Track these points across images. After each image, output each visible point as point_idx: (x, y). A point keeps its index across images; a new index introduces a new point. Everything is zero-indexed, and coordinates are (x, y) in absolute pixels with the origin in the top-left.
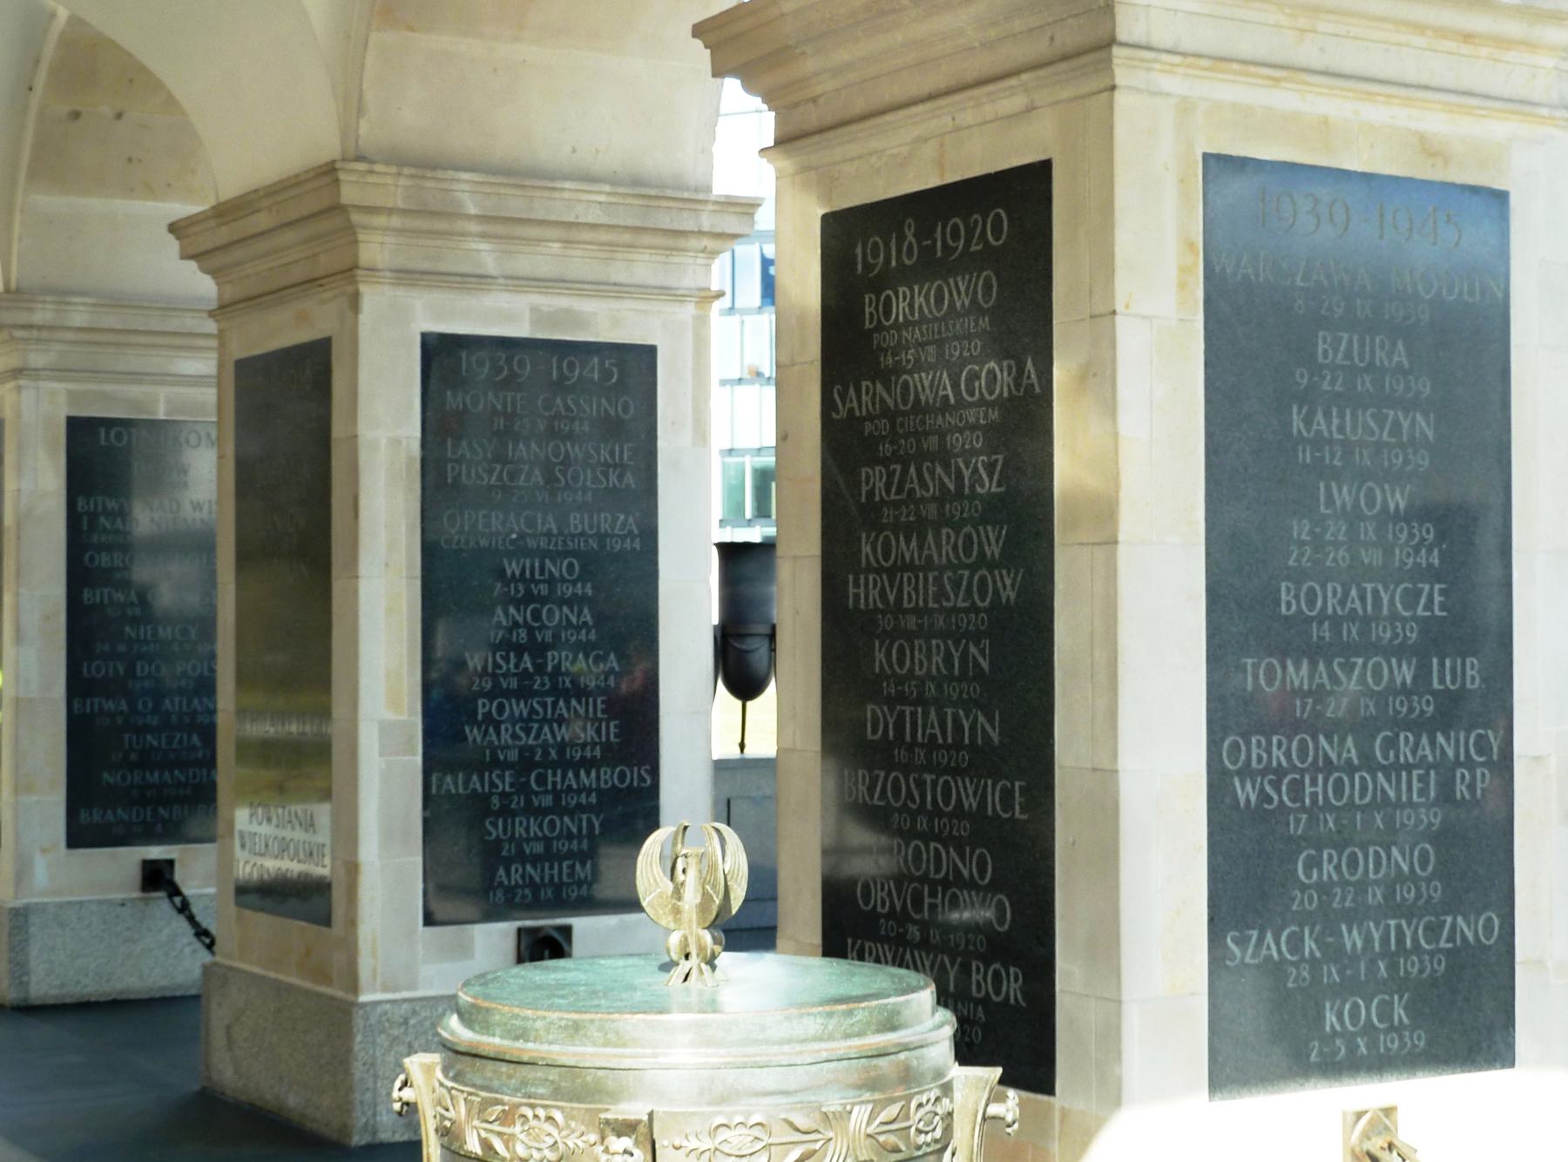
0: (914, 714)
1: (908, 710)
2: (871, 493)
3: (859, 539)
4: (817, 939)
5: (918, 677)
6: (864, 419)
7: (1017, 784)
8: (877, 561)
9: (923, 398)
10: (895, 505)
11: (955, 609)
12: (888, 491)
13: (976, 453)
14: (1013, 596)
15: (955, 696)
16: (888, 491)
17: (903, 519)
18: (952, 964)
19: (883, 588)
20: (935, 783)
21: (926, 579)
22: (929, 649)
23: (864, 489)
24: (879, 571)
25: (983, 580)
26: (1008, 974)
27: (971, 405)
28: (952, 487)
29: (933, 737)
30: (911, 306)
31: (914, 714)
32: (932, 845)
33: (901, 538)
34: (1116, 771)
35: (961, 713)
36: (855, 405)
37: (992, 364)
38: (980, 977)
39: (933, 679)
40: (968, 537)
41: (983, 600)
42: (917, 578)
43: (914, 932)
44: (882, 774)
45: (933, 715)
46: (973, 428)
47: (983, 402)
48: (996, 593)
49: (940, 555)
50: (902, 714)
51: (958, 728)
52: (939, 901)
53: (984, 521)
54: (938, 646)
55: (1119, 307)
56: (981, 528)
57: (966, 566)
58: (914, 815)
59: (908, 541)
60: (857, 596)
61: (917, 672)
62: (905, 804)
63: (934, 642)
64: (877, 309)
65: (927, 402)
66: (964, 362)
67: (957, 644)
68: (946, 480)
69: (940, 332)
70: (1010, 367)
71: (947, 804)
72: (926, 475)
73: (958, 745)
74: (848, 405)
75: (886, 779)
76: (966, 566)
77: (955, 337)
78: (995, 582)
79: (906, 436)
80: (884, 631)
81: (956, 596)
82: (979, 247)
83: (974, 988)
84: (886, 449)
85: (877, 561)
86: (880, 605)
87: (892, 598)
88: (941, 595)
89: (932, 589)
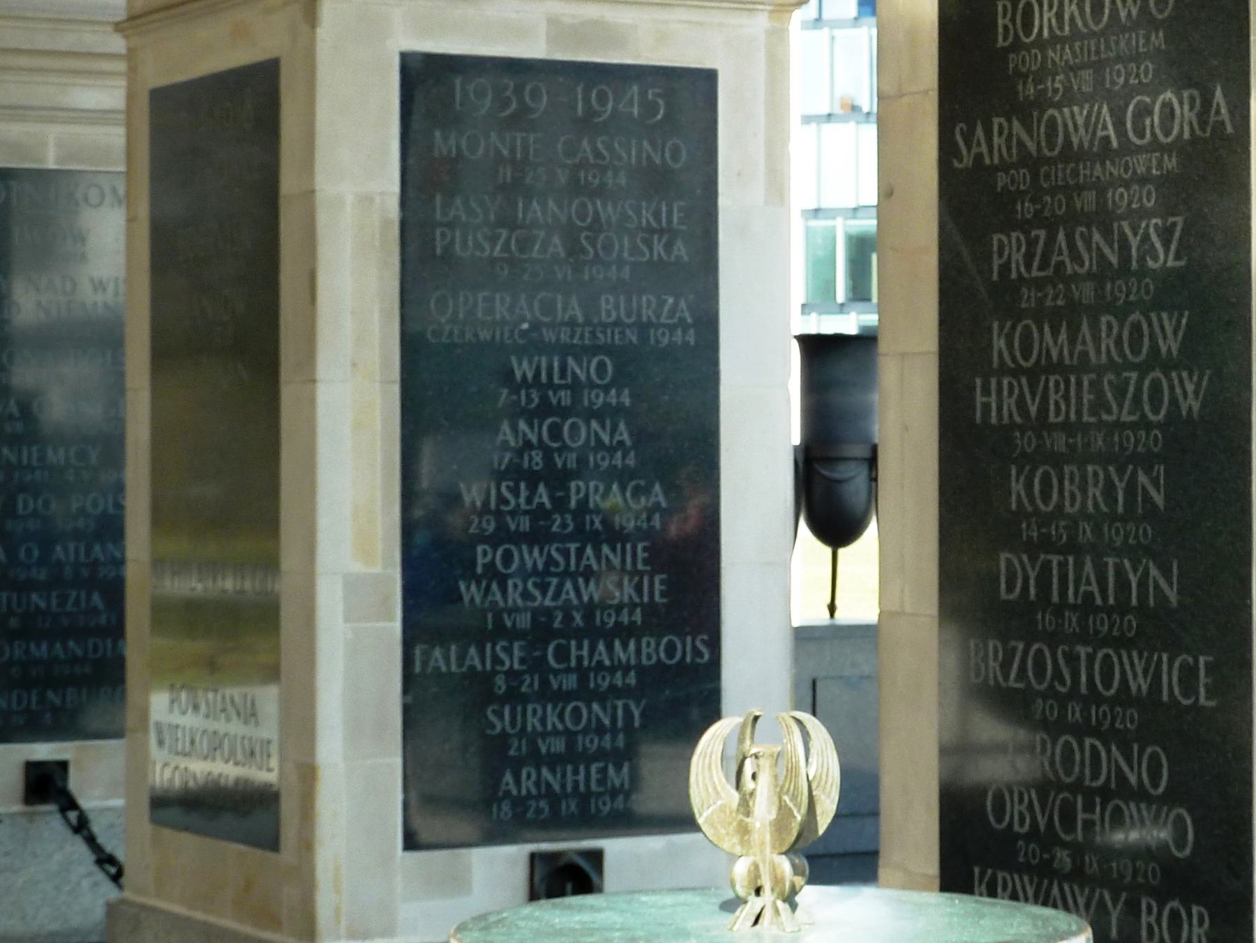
0: (1063, 565)
1: (1055, 559)
2: (1006, 268)
3: (990, 330)
4: (932, 868)
6: (997, 169)
7: (1202, 660)
8: (1014, 359)
9: (1075, 140)
10: (1039, 284)
11: (1119, 425)
12: (1028, 266)
13: (1148, 214)
14: (1196, 406)
15: (1119, 542)
16: (1028, 266)
17: (1049, 303)
18: (1115, 901)
19: (1021, 395)
20: (1091, 658)
21: (1079, 384)
22: (1084, 478)
23: (996, 263)
24: (1016, 372)
25: (1156, 388)
26: (1190, 915)
27: (1140, 149)
28: (1114, 260)
29: (1089, 596)
30: (1059, 16)
31: (1063, 565)
32: (1088, 742)
33: (1047, 329)
35: (1127, 563)
36: (984, 149)
37: (1169, 95)
39: (1088, 518)
40: (1136, 328)
41: (1156, 411)
42: (1067, 382)
43: (1063, 858)
44: (1021, 646)
45: (1088, 567)
46: (1143, 180)
47: (1155, 145)
48: (1174, 402)
49: (1098, 351)
50: (1046, 567)
52: (1097, 816)
53: (1158, 305)
54: (1096, 474)
56: (1153, 316)
57: (1134, 367)
58: (1063, 701)
59: (1055, 332)
60: (986, 407)
61: (1068, 509)
62: (1051, 686)
63: (1090, 468)
64: (1013, 20)
65: (1081, 145)
66: (1129, 91)
67: (1121, 471)
68: (1107, 251)
69: (1098, 52)
70: (1192, 99)
71: (1108, 686)
72: (1080, 244)
73: (1123, 607)
74: (974, 150)
76: (1134, 367)
77: (1119, 59)
78: (1172, 388)
79: (1053, 191)
81: (1121, 406)
84: (1026, 209)
85: (1014, 359)
86: (1018, 419)
87: (1033, 410)
88: (1100, 404)
89: (1087, 397)
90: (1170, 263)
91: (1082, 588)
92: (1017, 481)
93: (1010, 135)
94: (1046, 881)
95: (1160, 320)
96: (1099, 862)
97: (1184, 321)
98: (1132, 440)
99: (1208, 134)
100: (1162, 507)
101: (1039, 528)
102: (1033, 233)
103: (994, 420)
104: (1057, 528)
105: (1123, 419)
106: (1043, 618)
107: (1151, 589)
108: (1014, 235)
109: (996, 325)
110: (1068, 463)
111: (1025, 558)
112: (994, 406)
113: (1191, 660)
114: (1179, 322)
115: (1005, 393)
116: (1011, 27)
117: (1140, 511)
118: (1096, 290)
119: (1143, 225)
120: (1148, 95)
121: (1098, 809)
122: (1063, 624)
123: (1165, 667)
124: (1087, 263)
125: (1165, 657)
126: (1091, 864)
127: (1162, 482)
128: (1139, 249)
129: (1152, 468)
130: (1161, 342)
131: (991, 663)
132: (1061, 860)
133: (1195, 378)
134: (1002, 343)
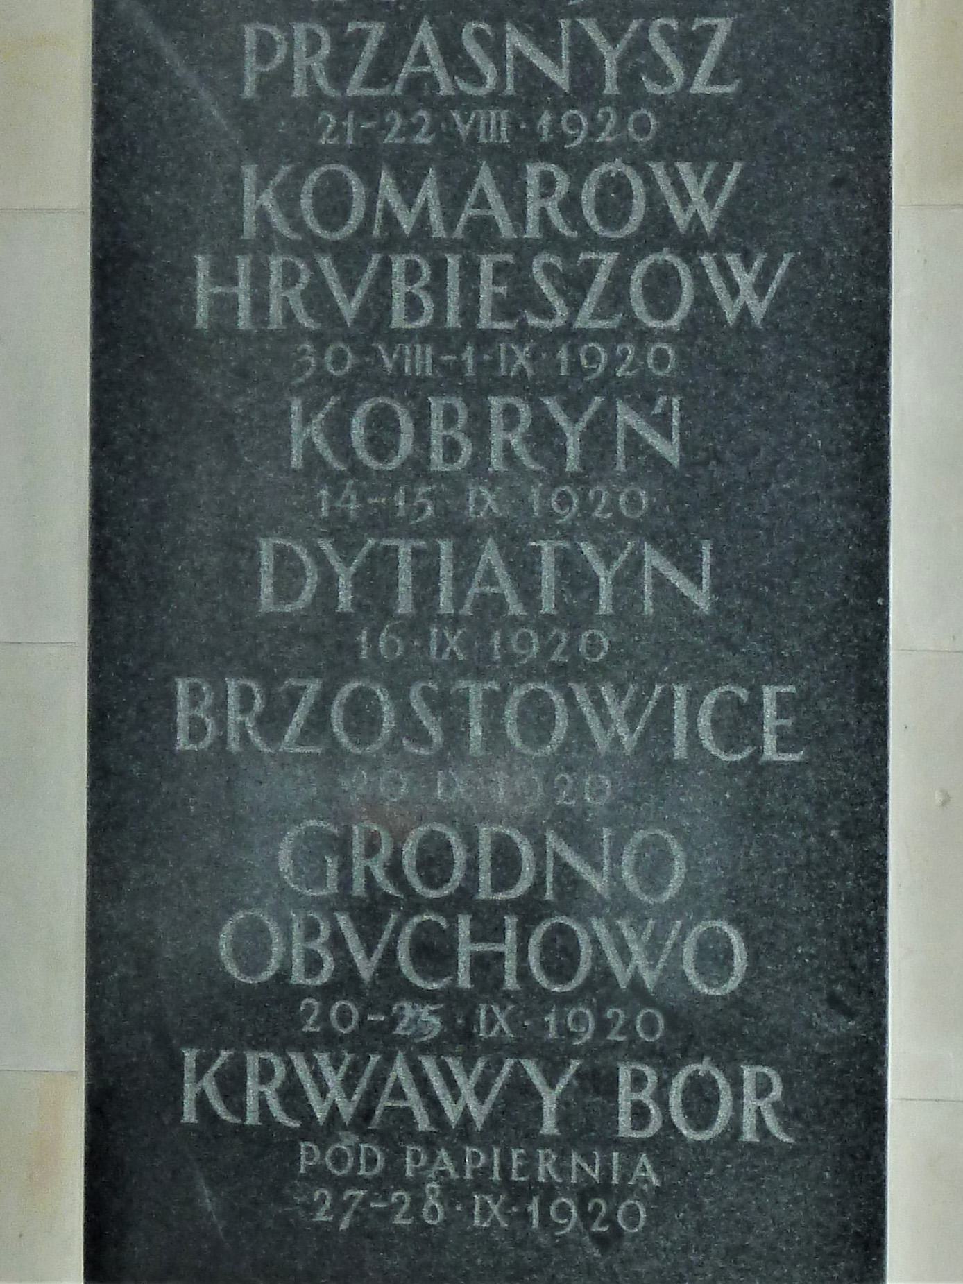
3: (236, 179)
5: (443, 477)
7: (768, 692)
10: (364, 108)
11: (569, 334)
14: (758, 310)
20: (495, 702)
21: (470, 272)
24: (309, 247)
28: (561, 78)
29: (492, 606)
35: (587, 549)
38: (645, 1096)
48: (705, 298)
49: (519, 218)
51: (573, 574)
52: (509, 945)
53: (667, 150)
57: (610, 245)
67: (574, 407)
72: (473, 49)
75: (324, 700)
80: (321, 378)
85: (299, 225)
86: (307, 322)
88: (520, 298)
90: (700, 86)
91: (474, 591)
92: (306, 420)
94: (374, 1059)
96: (511, 1020)
97: (732, 178)
98: (604, 357)
100: (676, 462)
101: (362, 499)
102: (351, 27)
104: (410, 496)
105: (578, 325)
106: (373, 640)
107: (648, 589)
108: (300, 30)
109: (250, 173)
110: (439, 392)
111: (326, 546)
112: (244, 301)
115: (275, 279)
117: (621, 467)
118: (514, 124)
119: (634, 25)
121: (510, 935)
122: (426, 646)
123: (680, 705)
124: (491, 81)
125: (680, 692)
126: (491, 1023)
127: (675, 422)
128: (621, 63)
129: (651, 400)
130: (675, 208)
131: (234, 716)
132: (415, 1020)
133: (757, 265)
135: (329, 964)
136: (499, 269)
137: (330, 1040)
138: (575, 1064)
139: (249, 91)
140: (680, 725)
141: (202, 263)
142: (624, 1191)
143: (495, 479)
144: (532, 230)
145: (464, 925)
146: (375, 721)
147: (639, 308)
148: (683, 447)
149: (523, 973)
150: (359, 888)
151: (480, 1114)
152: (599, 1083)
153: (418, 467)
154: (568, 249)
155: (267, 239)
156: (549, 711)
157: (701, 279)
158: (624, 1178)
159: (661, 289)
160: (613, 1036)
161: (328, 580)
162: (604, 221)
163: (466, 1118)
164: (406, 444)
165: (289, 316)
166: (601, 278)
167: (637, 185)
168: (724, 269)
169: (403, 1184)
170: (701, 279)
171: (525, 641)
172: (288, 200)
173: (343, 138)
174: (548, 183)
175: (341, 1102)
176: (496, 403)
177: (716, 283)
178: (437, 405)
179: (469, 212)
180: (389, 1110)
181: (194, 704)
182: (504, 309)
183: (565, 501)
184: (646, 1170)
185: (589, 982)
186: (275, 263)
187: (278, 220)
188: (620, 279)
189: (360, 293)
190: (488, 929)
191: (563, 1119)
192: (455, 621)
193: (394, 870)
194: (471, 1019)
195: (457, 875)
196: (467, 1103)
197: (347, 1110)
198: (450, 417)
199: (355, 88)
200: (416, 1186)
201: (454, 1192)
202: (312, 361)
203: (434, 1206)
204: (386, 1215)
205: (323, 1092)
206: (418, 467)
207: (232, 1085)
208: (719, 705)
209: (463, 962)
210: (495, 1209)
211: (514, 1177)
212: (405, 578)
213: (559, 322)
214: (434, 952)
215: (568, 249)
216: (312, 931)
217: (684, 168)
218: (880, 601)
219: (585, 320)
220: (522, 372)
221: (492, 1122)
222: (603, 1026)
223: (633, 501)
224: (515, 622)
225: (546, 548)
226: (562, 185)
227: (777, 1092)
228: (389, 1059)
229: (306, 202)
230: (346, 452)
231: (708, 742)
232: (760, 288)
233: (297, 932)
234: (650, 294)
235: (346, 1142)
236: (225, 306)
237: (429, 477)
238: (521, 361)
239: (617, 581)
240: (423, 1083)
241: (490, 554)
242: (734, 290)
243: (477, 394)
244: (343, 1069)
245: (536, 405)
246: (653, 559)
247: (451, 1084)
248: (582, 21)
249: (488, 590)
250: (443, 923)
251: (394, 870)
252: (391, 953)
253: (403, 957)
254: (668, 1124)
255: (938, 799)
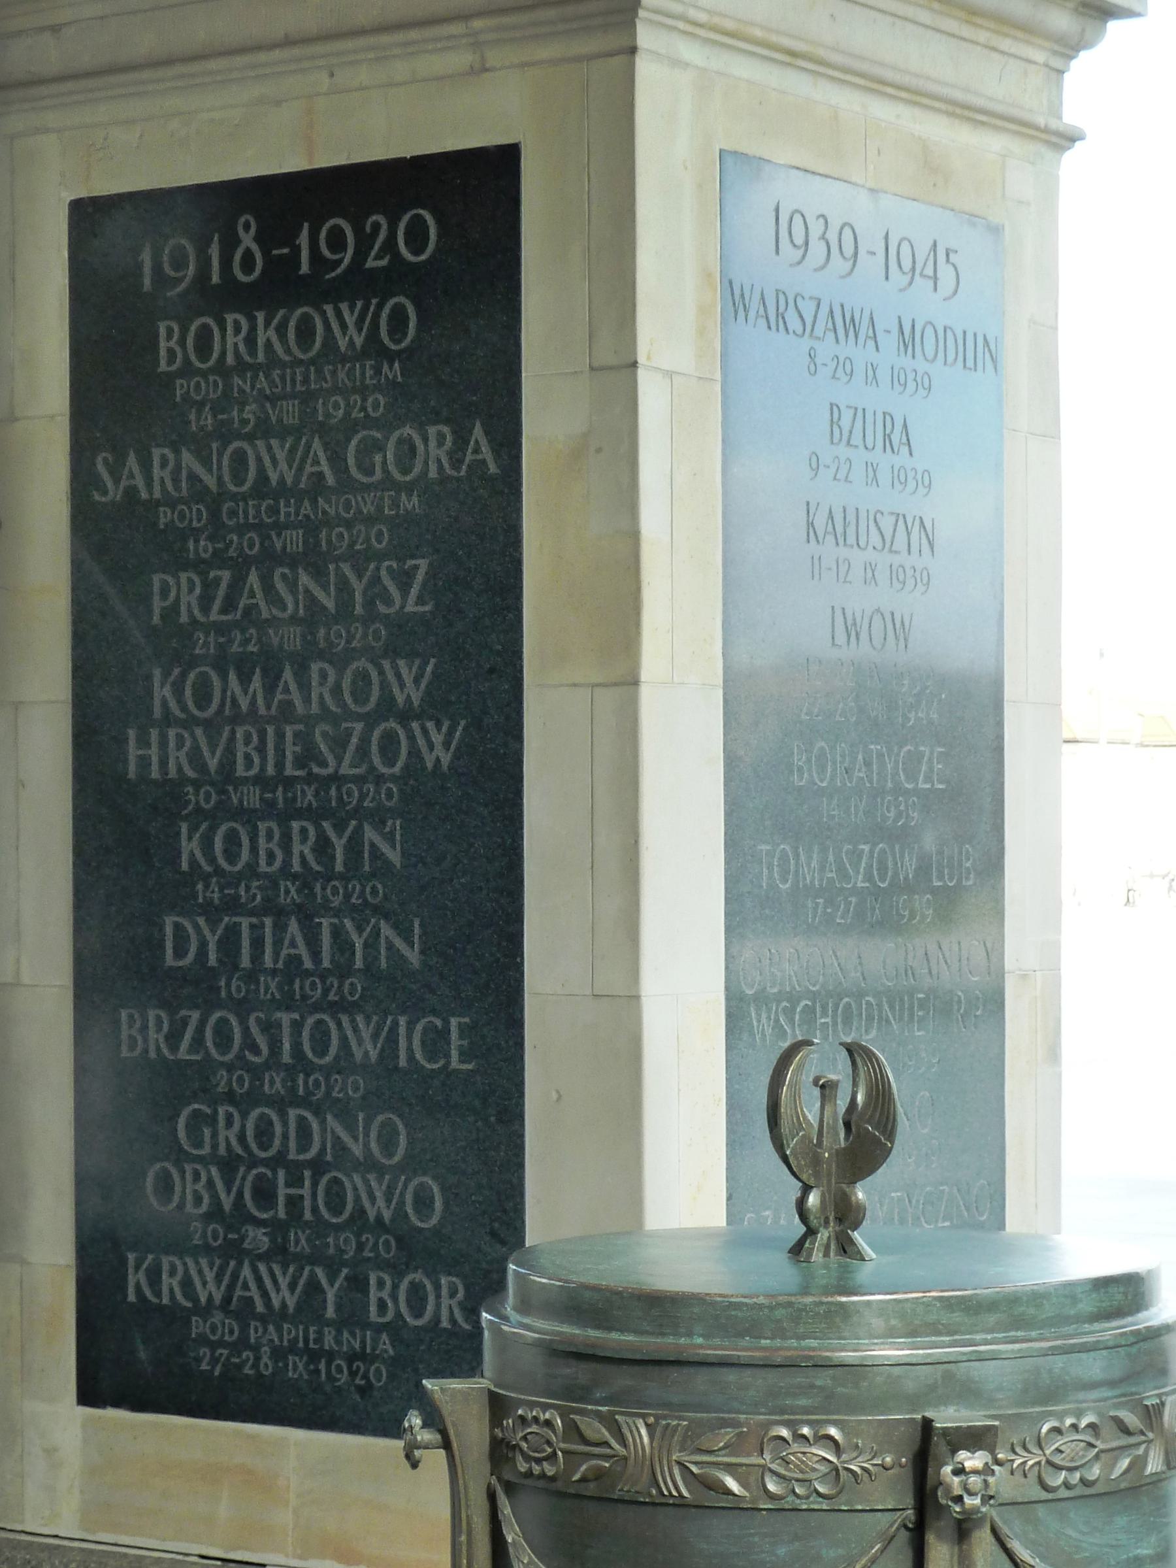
1: (245, 922)
3: (149, 677)
5: (266, 875)
6: (158, 503)
7: (454, 1021)
9: (274, 477)
10: (220, 629)
11: (336, 778)
13: (381, 557)
14: (446, 759)
15: (336, 902)
16: (205, 609)
17: (235, 648)
20: (297, 1026)
21: (280, 736)
23: (157, 604)
24: (189, 723)
25: (389, 739)
26: (437, 1287)
28: (330, 604)
29: (294, 960)
32: (292, 1113)
34: (636, 998)
35: (348, 923)
38: (385, 1294)
39: (295, 877)
44: (195, 1015)
46: (370, 520)
48: (414, 753)
49: (307, 700)
50: (233, 932)
51: (342, 943)
52: (306, 1191)
53: (392, 651)
54: (304, 831)
55: (641, 359)
56: (386, 664)
57: (359, 717)
58: (256, 1072)
61: (263, 867)
62: (240, 1057)
64: (182, 342)
65: (282, 481)
66: (350, 427)
67: (340, 828)
69: (306, 381)
72: (280, 586)
73: (343, 970)
74: (124, 483)
75: (202, 1023)
76: (359, 717)
77: (336, 390)
79: (241, 529)
80: (198, 810)
82: (384, 263)
83: (373, 1309)
84: (204, 547)
85: (184, 708)
86: (190, 773)
88: (308, 756)
90: (410, 608)
91: (284, 952)
92: (190, 838)
93: (178, 468)
94: (232, 1263)
95: (395, 668)
96: (308, 1240)
97: (429, 669)
98: (356, 794)
99: (463, 473)
100: (398, 866)
101: (221, 890)
102: (212, 574)
103: (155, 774)
104: (248, 888)
105: (342, 771)
106: (228, 985)
107: (383, 951)
108: (184, 576)
109: (157, 673)
110: (262, 819)
111: (201, 921)
112: (155, 759)
113: (439, 1023)
114: (422, 669)
115: (172, 744)
116: (178, 350)
117: (367, 868)
118: (303, 636)
119: (372, 566)
120: (378, 430)
121: (307, 1183)
122: (257, 990)
123: (402, 1030)
124: (290, 606)
125: (402, 1021)
126: (297, 1242)
127: (398, 837)
128: (364, 593)
129: (383, 822)
130: (396, 690)
131: (152, 1034)
132: (254, 1239)
133: (444, 729)
134: (167, 691)
135: (206, 1200)
136: (296, 735)
137: (207, 1249)
138: (345, 1271)
139: (156, 619)
140: (402, 1043)
141: (132, 734)
142: (374, 1358)
143: (295, 877)
144: (315, 708)
145: (281, 1174)
146: (230, 1039)
147: (377, 760)
148: (403, 853)
149: (315, 1210)
150: (222, 1150)
151: (291, 1303)
152: (358, 1284)
153: (252, 870)
154: (335, 720)
155: (168, 720)
156: (327, 1033)
157: (411, 738)
158: (374, 1349)
159: (389, 744)
160: (367, 1254)
161: (203, 944)
162: (356, 701)
163: (284, 1305)
164: (245, 855)
165: (180, 769)
166: (354, 740)
167: (374, 675)
168: (425, 732)
169: (249, 1347)
170: (411, 738)
171: (313, 986)
172: (178, 691)
173: (209, 649)
174: (323, 676)
175: (213, 1289)
176: (295, 825)
177: (421, 742)
178: (262, 826)
179: (279, 696)
180: (241, 1298)
181: (130, 1027)
182: (300, 762)
183: (335, 891)
184: (385, 1344)
185: (352, 1216)
186: (172, 733)
187: (173, 705)
188: (365, 740)
189: (218, 754)
190: (295, 1181)
191: (339, 1308)
192: (274, 972)
193: (242, 1138)
194: (286, 1239)
195: (277, 1142)
196: (285, 1297)
197: (218, 1298)
198: (270, 836)
199: (214, 616)
200: (256, 1349)
201: (278, 1354)
202: (193, 798)
203: (267, 1365)
204: (239, 1367)
205: (204, 1284)
206: (252, 870)
207: (154, 1277)
208: (425, 1031)
209: (281, 1200)
210: (301, 1366)
211: (311, 1345)
212: (246, 943)
213: (330, 770)
214: (265, 1194)
215: (335, 720)
216: (197, 1176)
217: (401, 663)
218: (518, 960)
219: (345, 770)
220: (310, 804)
221: (299, 1308)
222: (360, 1247)
223: (374, 891)
224: (308, 974)
225: (325, 922)
226: (331, 679)
227: (461, 1295)
228: (240, 1264)
229: (188, 692)
230: (212, 860)
231: (419, 1056)
232: (447, 745)
233: (189, 1176)
234: (383, 750)
235: (217, 1317)
236: (144, 762)
237: (258, 876)
238: (310, 797)
239: (366, 945)
240: (259, 1280)
241: (293, 927)
242: (431, 747)
243: (284, 819)
244: (215, 1269)
245: (318, 827)
246: (386, 930)
247: (275, 1282)
248: (341, 565)
249: (292, 951)
250: (269, 1174)
251: (242, 1138)
252: (240, 1194)
253: (247, 1195)
254: (399, 1315)
255: (554, 1096)
